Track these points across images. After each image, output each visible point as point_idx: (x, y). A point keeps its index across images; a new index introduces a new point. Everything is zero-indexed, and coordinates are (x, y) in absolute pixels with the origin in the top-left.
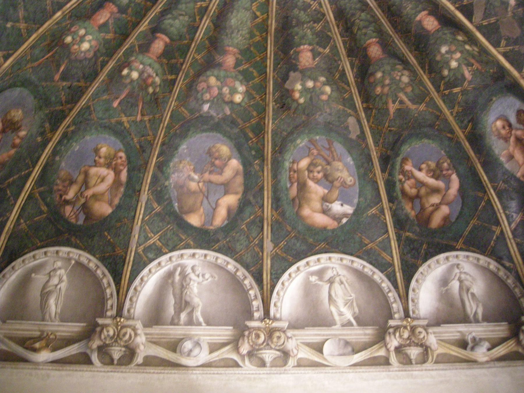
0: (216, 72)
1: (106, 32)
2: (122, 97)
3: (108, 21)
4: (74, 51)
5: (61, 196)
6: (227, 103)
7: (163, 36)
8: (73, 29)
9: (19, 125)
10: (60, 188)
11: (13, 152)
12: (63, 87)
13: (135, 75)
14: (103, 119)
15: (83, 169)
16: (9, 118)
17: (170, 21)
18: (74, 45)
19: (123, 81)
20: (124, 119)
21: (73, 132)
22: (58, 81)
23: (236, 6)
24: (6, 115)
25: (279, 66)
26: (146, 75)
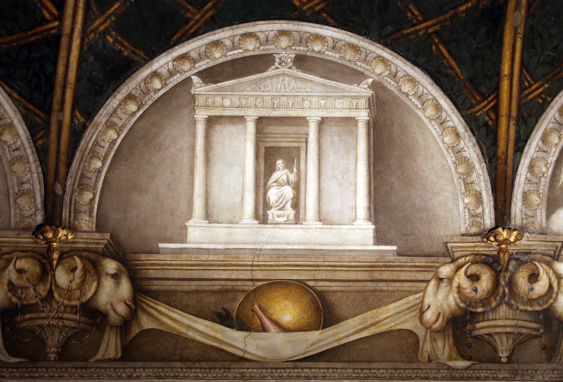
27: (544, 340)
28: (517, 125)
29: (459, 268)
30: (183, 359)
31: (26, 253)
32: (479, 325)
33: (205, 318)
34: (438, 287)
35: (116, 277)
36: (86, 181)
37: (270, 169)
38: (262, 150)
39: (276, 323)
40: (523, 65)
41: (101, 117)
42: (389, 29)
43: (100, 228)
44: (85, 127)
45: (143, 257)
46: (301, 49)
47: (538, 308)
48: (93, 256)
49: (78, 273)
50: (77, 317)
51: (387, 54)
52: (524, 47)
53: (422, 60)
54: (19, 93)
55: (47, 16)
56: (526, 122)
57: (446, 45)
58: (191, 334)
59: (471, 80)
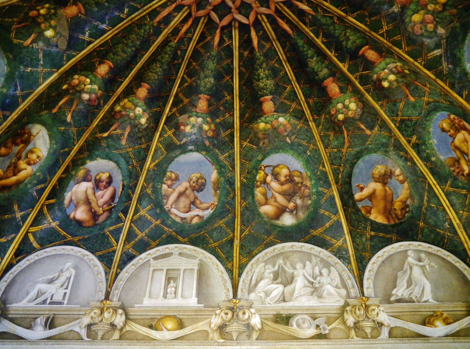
0: (410, 13)
1: (347, 89)
2: (408, 92)
3: (338, 86)
4: (353, 115)
5: (463, 175)
6: (444, 10)
7: (363, 49)
8: (333, 113)
9: (389, 172)
10: (457, 171)
11: (406, 185)
12: (378, 131)
13: (392, 77)
14: (421, 113)
15: (453, 147)
16: (377, 176)
17: (349, 43)
18: (347, 114)
19: (394, 87)
20: (426, 99)
21: (418, 139)
22: (372, 132)
26: (394, 70)
27: (247, 333)
28: (239, 269)
29: (222, 311)
30: (137, 340)
31: (98, 308)
32: (227, 328)
33: (145, 327)
34: (215, 317)
35: (121, 314)
36: (118, 288)
37: (169, 283)
38: (167, 278)
39: (166, 328)
40: (240, 254)
41: (125, 270)
42: (205, 245)
43: (119, 300)
44: (120, 273)
45: (130, 309)
46: (181, 251)
47: (245, 323)
48: (116, 309)
49: (111, 313)
50: (108, 327)
51: (204, 252)
52: (240, 249)
53: (213, 253)
54: (105, 265)
55: (114, 245)
56: (241, 269)
58: (140, 332)
59: (226, 258)
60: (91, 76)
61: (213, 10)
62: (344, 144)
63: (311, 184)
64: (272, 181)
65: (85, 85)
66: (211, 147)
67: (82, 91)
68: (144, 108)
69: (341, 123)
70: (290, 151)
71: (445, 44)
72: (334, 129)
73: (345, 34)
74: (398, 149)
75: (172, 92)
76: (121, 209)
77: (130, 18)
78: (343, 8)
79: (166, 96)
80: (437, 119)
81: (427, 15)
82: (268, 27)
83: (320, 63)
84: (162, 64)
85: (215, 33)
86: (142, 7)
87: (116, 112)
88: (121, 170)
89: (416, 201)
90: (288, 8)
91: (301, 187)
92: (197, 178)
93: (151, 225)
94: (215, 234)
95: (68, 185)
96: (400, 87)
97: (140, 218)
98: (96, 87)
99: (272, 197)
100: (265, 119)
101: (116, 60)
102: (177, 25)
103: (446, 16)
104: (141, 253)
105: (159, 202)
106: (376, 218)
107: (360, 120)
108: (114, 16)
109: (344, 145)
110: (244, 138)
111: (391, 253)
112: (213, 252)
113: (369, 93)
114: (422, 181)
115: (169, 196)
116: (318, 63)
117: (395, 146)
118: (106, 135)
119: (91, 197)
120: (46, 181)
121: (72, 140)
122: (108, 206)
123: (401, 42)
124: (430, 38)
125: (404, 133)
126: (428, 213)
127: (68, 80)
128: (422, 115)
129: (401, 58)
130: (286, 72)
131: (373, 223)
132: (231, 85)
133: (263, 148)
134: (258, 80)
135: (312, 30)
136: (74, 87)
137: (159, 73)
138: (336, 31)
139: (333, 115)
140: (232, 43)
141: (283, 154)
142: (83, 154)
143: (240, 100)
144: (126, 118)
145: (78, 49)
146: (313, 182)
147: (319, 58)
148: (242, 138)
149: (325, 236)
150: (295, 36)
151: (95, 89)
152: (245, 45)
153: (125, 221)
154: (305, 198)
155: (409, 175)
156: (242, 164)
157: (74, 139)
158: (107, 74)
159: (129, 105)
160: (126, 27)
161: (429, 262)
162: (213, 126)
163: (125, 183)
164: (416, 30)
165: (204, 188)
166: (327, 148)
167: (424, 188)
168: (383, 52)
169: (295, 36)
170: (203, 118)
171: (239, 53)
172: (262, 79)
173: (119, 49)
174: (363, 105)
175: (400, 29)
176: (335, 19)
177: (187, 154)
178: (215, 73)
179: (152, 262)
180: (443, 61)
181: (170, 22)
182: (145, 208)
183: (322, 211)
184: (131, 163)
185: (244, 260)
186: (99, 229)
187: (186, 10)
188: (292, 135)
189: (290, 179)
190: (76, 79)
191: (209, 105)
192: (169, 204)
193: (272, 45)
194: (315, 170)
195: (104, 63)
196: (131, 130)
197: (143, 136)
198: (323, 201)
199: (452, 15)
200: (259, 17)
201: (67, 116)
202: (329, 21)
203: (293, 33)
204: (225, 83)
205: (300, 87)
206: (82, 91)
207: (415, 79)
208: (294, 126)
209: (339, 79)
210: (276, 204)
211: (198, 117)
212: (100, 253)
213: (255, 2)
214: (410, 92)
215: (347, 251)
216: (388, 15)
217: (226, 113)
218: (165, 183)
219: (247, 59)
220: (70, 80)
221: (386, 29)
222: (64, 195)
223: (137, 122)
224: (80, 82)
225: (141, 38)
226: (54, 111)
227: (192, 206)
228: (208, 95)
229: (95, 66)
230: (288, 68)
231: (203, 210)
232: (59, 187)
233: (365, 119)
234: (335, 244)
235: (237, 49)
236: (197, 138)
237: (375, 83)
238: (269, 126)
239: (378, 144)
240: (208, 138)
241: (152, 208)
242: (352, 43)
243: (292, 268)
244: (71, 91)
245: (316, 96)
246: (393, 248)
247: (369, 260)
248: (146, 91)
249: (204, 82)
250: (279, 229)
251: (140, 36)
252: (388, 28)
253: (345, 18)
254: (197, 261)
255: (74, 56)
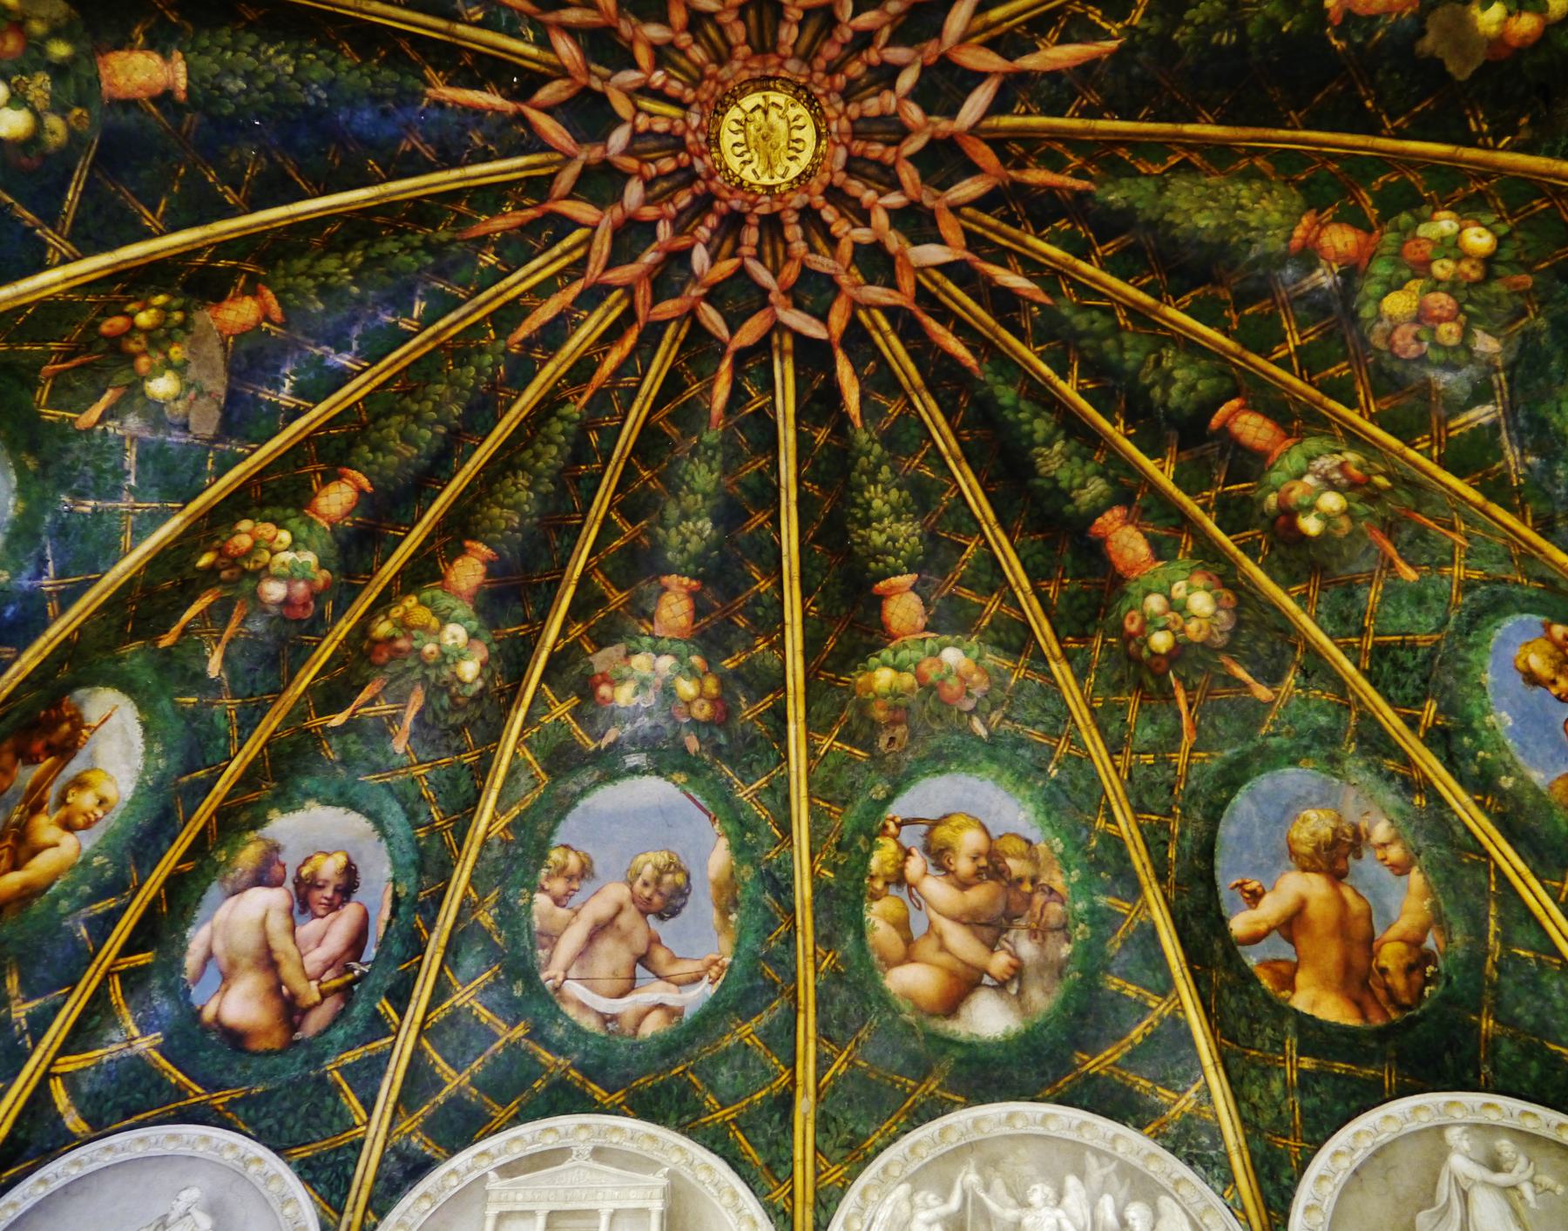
0: (1373, 288)
1: (1177, 547)
2: (1391, 550)
3: (1146, 535)
6: (1489, 276)
7: (1223, 410)
8: (1132, 627)
9: (1348, 831)
11: (1416, 878)
12: (1297, 686)
13: (1332, 501)
14: (1446, 621)
16: (1307, 849)
17: (1175, 391)
18: (1183, 630)
19: (1340, 534)
20: (1458, 572)
21: (1446, 710)
23: (1152, 214)
24: (1293, 854)
25: (1369, 104)
26: (1337, 475)
40: (816, 1149)
42: (687, 1118)
46: (600, 1142)
53: (718, 1147)
55: (358, 1122)
56: (824, 1207)
57: (742, 1130)
59: (768, 1165)
60: (293, 523)
61: (707, 298)
62: (1177, 735)
63: (1068, 884)
64: (926, 874)
65: (273, 553)
66: (707, 757)
67: (263, 574)
68: (474, 624)
69: (1164, 663)
70: (985, 764)
71: (1505, 388)
72: (1140, 685)
73: (1158, 362)
74: (1377, 752)
75: (569, 569)
76: (388, 983)
77: (430, 331)
78: (1145, 281)
79: (549, 583)
80: (1504, 641)
81: (1432, 296)
82: (893, 347)
83: (1076, 460)
84: (538, 476)
85: (716, 370)
86: (470, 298)
87: (376, 642)
88: (390, 844)
89: (1457, 938)
90: (957, 284)
91: (1031, 894)
92: (656, 867)
93: (493, 1042)
94: (724, 1075)
95: (199, 900)
96: (1362, 533)
97: (453, 1019)
98: (310, 558)
99: (927, 934)
100: (895, 655)
101: (382, 466)
102: (587, 351)
103: (1497, 295)
104: (453, 1152)
105: (523, 959)
106: (1314, 1004)
107: (1229, 649)
108: (379, 328)
109: (1179, 740)
110: (822, 722)
111: (1384, 1138)
112: (718, 1142)
113: (1254, 558)
114: (1475, 865)
115: (558, 937)
116: (1069, 459)
117: (1361, 739)
118: (338, 720)
119: (281, 943)
120: (126, 888)
121: (222, 742)
122: (339, 976)
123: (1353, 383)
124: (1455, 368)
125: (1391, 691)
126: (1508, 982)
127: (218, 538)
128: (1451, 627)
129: (1358, 438)
130: (961, 495)
131: (1305, 1023)
132: (774, 543)
133: (889, 758)
134: (866, 523)
135: (1042, 352)
136: (234, 561)
137: (527, 508)
138: (1127, 356)
139: (1132, 636)
140: (773, 402)
141: (962, 778)
142: (259, 789)
143: (806, 592)
144: (410, 663)
145: (254, 434)
146: (1075, 875)
147: (1073, 443)
148: (813, 724)
149: (1132, 1077)
150: (985, 373)
151: (305, 565)
152: (817, 407)
153: (399, 1029)
154: (1050, 936)
155: (1423, 844)
156: (815, 816)
157: (229, 738)
158: (348, 514)
159: (422, 615)
160: (416, 362)
161: (1530, 1172)
162: (711, 685)
163: (403, 890)
164: (1400, 343)
165: (683, 905)
166: (1120, 753)
167: (1482, 891)
168: (1293, 418)
169: (985, 373)
170: (676, 656)
171: (799, 433)
172: (880, 519)
173: (393, 431)
174: (1239, 598)
175: (1343, 342)
176: (1121, 315)
177: (619, 783)
178: (718, 501)
179: (495, 1183)
180: (1506, 442)
181: (564, 340)
182: (470, 981)
183: (1114, 983)
184: (423, 818)
185: (835, 1174)
186: (306, 1062)
187: (618, 302)
188: (993, 709)
189: (992, 866)
190: (244, 534)
191: (699, 611)
192: (555, 967)
193: (911, 405)
194: (1078, 832)
195: (339, 478)
196: (428, 702)
197: (466, 722)
198: (1114, 945)
199: (1520, 294)
200: (862, 315)
201: (207, 659)
202: (1101, 324)
203: (980, 364)
204: (751, 534)
205: (1011, 542)
206: (263, 573)
207: (1413, 506)
208: (996, 679)
209: (1146, 510)
210: (943, 958)
211: (659, 653)
212: (306, 1152)
213: (847, 271)
214: (1399, 551)
215: (1217, 1136)
216: (1301, 298)
217: (755, 636)
218: (543, 890)
219: (826, 452)
220: (224, 537)
221: (1298, 342)
222: (183, 937)
223: (446, 673)
224: (256, 544)
225: (467, 394)
226: (166, 641)
227: (639, 968)
228: (692, 578)
229: (311, 488)
230: (967, 480)
231: (678, 984)
232: (170, 907)
233: (1248, 648)
234: (1169, 1108)
235: (791, 421)
236: (655, 727)
237: (1274, 521)
238: (908, 679)
239: (1300, 735)
240: (696, 724)
241: (498, 981)
242: (1183, 393)
243: (1012, 1202)
244: (225, 574)
245: (1069, 573)
246: (1388, 1117)
247: (1304, 1166)
248: (481, 569)
249: (679, 532)
250: (958, 1053)
251: (463, 387)
252: (1302, 338)
253: (1155, 312)
254: (659, 1180)
255: (241, 458)
